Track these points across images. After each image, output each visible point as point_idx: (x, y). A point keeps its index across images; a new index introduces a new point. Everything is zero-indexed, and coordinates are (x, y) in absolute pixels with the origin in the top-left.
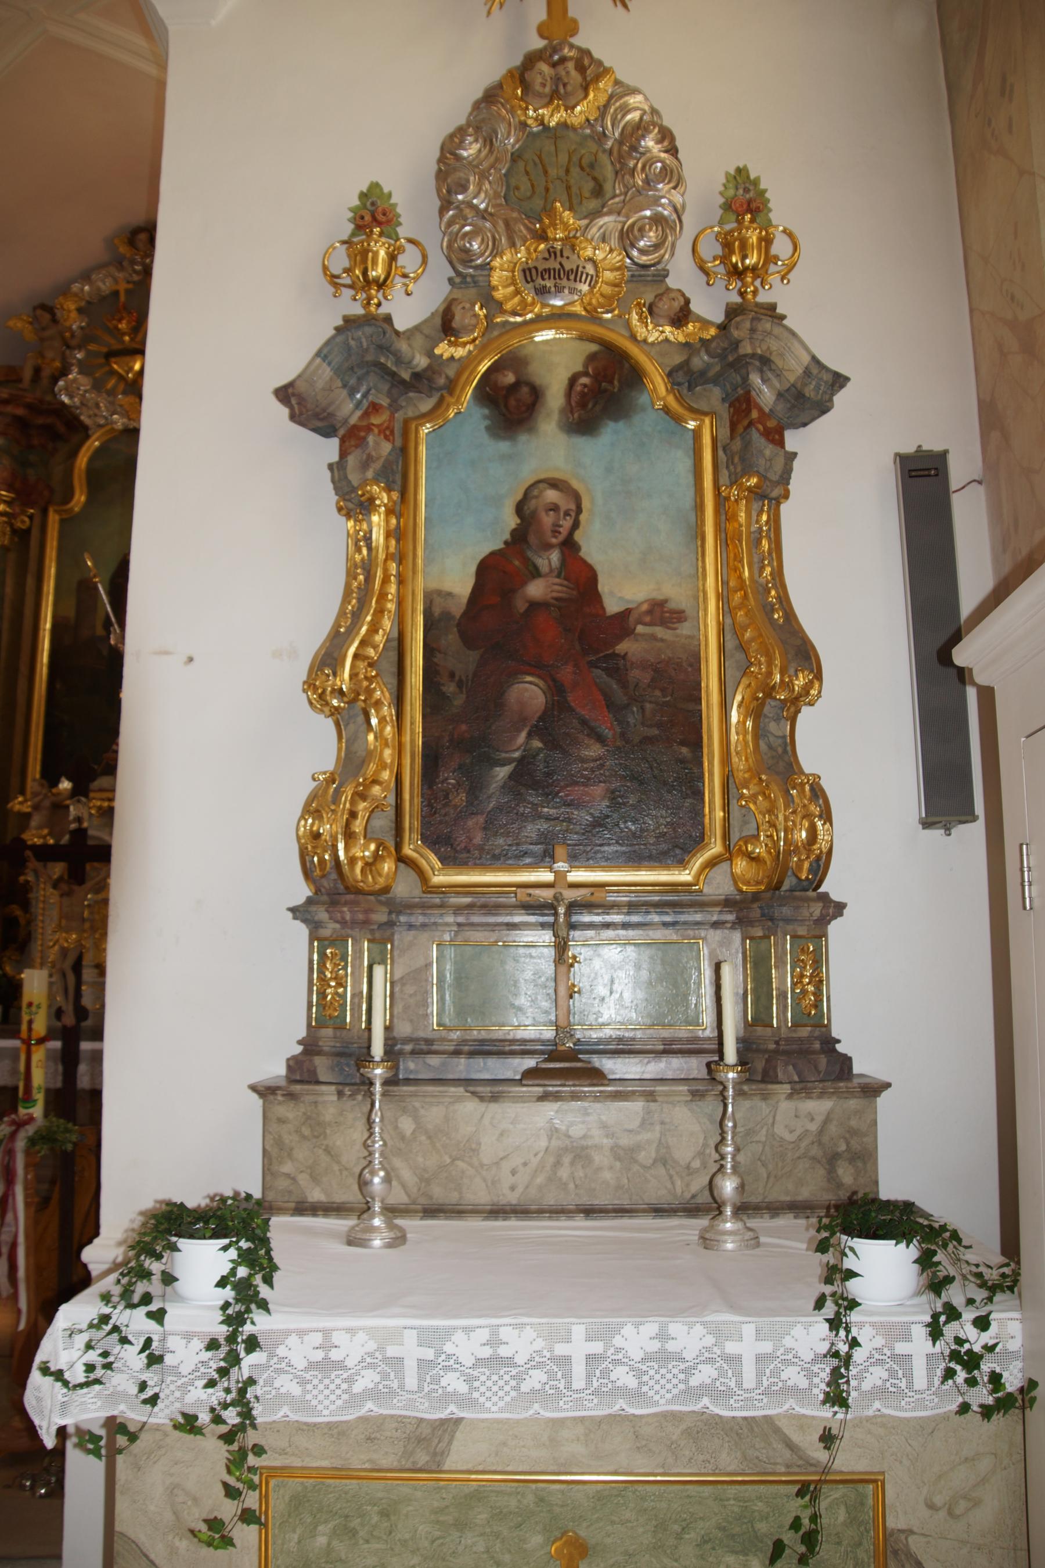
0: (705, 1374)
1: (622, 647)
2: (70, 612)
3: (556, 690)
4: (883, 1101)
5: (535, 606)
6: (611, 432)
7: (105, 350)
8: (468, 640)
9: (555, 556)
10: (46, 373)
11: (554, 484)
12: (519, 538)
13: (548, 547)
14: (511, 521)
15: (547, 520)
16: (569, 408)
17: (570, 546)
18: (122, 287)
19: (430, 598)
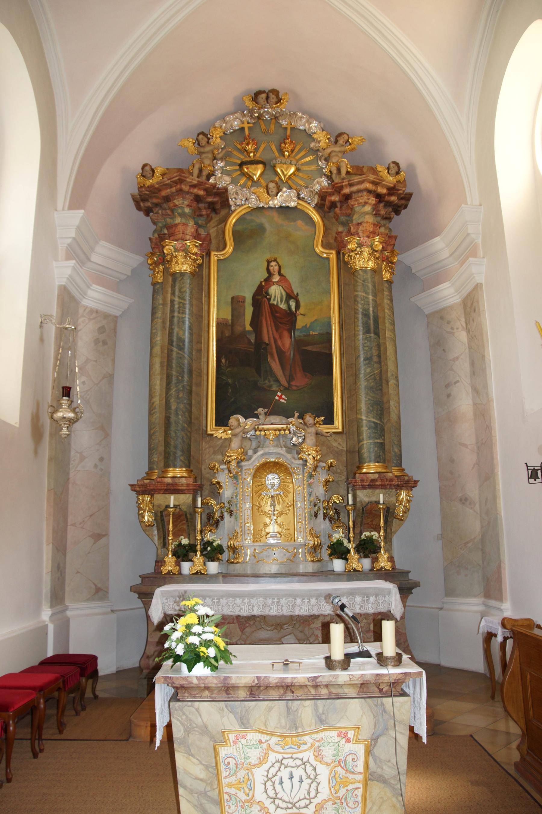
2: (228, 316)
7: (239, 162)
10: (205, 173)
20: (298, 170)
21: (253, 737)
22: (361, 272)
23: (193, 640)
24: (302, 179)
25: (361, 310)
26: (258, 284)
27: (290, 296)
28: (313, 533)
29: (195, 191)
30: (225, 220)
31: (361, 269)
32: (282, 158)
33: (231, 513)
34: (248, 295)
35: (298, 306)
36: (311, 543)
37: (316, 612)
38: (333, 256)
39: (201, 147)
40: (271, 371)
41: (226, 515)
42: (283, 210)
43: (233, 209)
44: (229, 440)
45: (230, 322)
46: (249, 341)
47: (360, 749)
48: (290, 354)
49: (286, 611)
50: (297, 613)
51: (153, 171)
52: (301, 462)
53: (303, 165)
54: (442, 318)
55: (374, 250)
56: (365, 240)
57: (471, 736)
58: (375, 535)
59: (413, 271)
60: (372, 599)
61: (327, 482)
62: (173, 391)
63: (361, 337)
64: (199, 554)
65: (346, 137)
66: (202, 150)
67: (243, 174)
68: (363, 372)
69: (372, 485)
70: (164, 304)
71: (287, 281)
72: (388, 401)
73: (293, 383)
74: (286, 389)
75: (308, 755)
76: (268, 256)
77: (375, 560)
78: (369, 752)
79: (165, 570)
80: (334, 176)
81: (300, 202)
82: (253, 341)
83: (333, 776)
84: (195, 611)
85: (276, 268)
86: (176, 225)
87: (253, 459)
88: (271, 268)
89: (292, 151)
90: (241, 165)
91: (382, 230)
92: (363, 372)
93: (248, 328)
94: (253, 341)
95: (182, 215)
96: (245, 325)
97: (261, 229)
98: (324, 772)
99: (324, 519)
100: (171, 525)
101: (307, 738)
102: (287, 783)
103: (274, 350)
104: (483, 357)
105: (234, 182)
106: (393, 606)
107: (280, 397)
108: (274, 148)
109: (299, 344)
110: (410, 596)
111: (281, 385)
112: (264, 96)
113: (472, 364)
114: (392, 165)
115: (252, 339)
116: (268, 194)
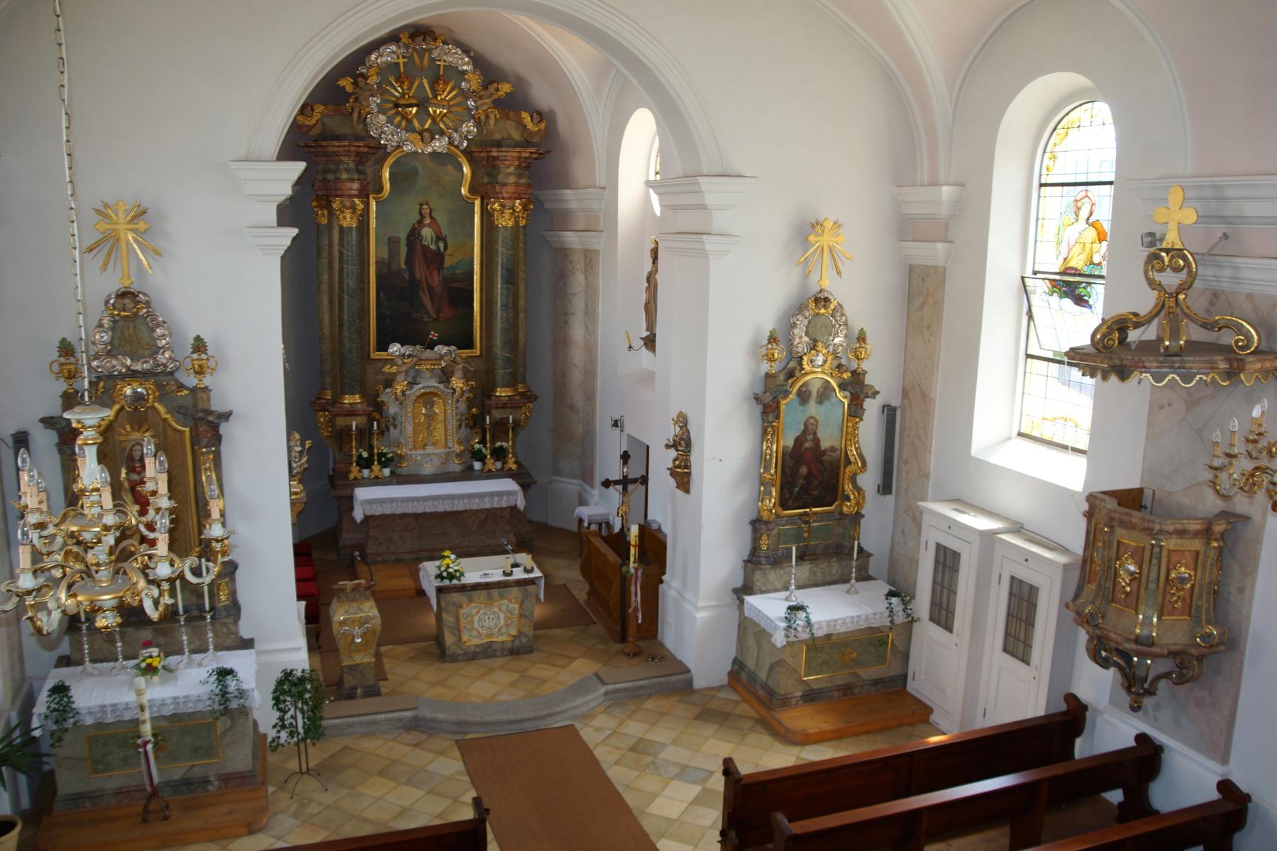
0: (872, 621)
1: (825, 458)
2: (385, 254)
3: (810, 469)
4: (871, 558)
5: (806, 449)
6: (826, 403)
8: (791, 458)
9: (811, 436)
10: (363, 116)
11: (812, 418)
12: (804, 432)
13: (810, 434)
14: (802, 427)
15: (810, 427)
16: (817, 397)
17: (815, 433)
18: (401, 61)
19: (784, 447)
20: (449, 112)
21: (473, 605)
22: (502, 229)
23: (451, 570)
24: (452, 121)
25: (500, 263)
26: (412, 225)
27: (440, 237)
28: (460, 443)
29: (361, 149)
30: (381, 162)
31: (503, 227)
32: (434, 101)
33: (395, 427)
34: (403, 236)
35: (446, 247)
36: (458, 451)
37: (468, 507)
38: (477, 203)
39: (361, 89)
40: (423, 305)
41: (392, 428)
42: (434, 154)
43: (388, 150)
44: (395, 374)
45: (387, 260)
46: (404, 277)
47: (517, 606)
48: (439, 289)
49: (449, 509)
50: (455, 509)
51: (313, 110)
52: (451, 391)
53: (454, 106)
54: (566, 256)
55: (514, 210)
56: (508, 203)
57: (564, 585)
58: (505, 444)
59: (547, 206)
60: (505, 498)
61: (468, 398)
62: (346, 333)
63: (499, 286)
64: (376, 463)
65: (496, 85)
66: (358, 90)
67: (398, 113)
68: (499, 315)
69: (504, 406)
70: (331, 245)
71: (437, 223)
72: (518, 333)
73: (441, 315)
74: (435, 320)
75: (496, 610)
76: (421, 199)
77: (504, 463)
78: (521, 606)
79: (352, 476)
80: (482, 124)
81: (451, 148)
82: (407, 278)
83: (506, 617)
84: (449, 557)
85: (428, 211)
86: (343, 181)
87: (414, 389)
88: (423, 211)
89: (444, 91)
90: (397, 106)
91: (523, 181)
92: (499, 315)
93: (403, 266)
94: (407, 278)
95: (348, 171)
96: (399, 264)
97: (414, 172)
98: (502, 616)
99: (466, 427)
100: (354, 444)
101: (496, 604)
102: (487, 620)
103: (425, 286)
104: (594, 309)
105: (390, 121)
106: (519, 503)
107: (433, 336)
108: (427, 86)
109: (447, 281)
110: (530, 490)
111: (430, 317)
112: (421, 38)
113: (586, 305)
114: (535, 115)
115: (407, 276)
116: (422, 141)
